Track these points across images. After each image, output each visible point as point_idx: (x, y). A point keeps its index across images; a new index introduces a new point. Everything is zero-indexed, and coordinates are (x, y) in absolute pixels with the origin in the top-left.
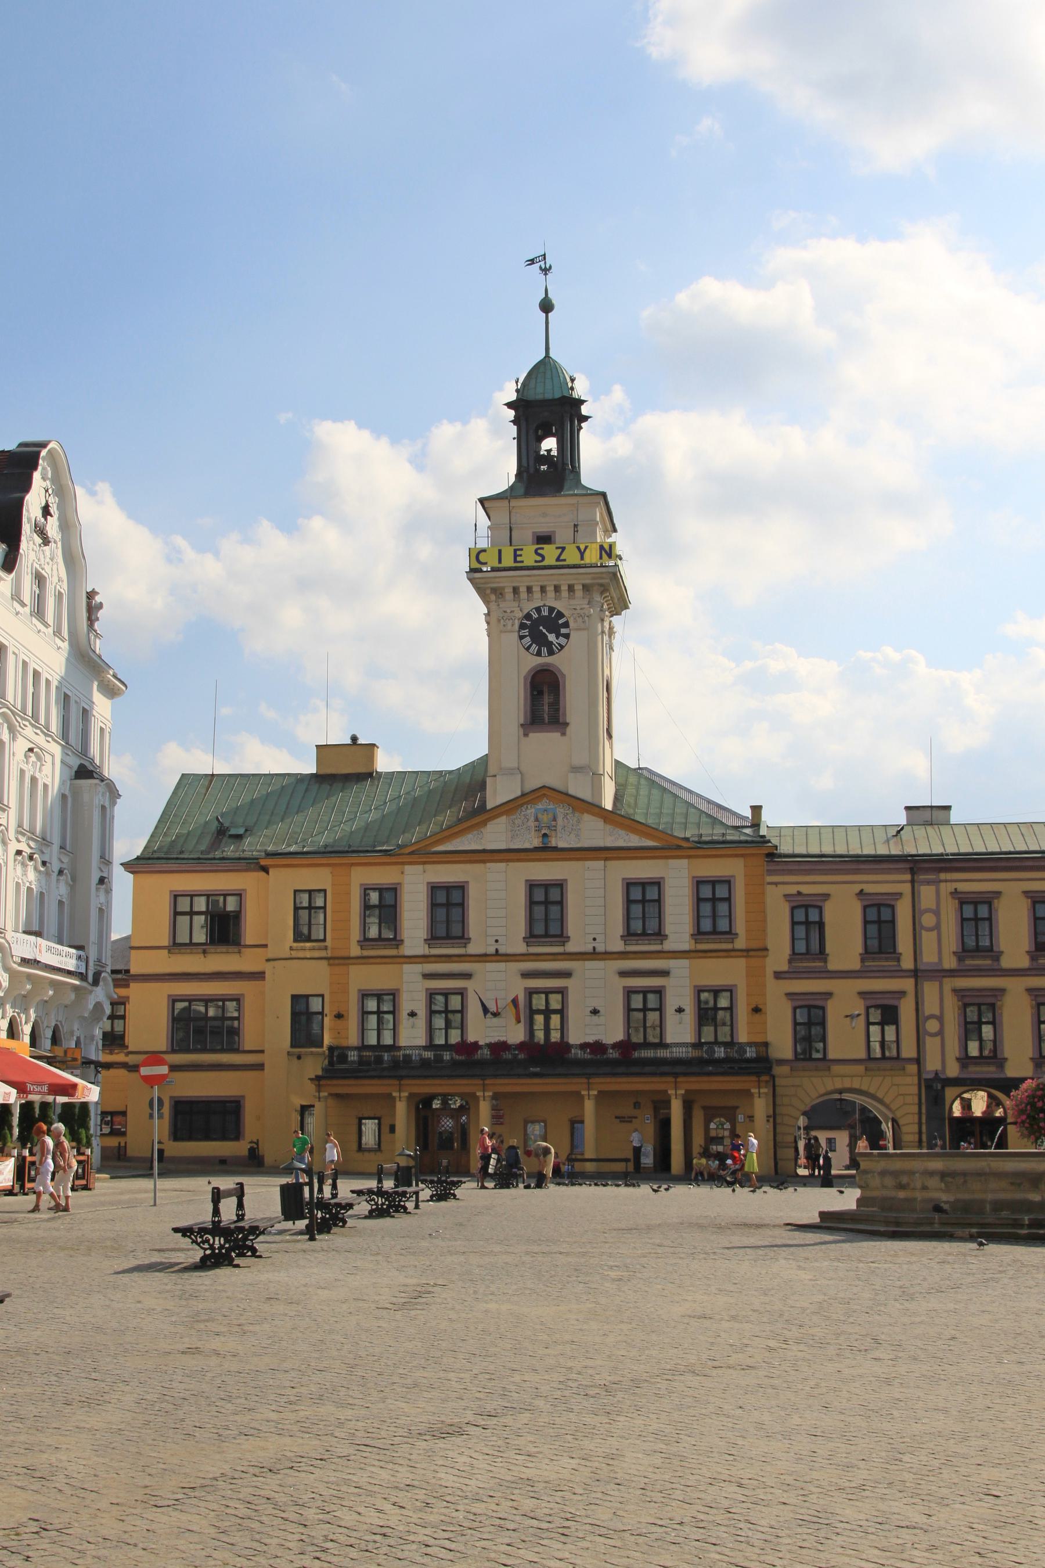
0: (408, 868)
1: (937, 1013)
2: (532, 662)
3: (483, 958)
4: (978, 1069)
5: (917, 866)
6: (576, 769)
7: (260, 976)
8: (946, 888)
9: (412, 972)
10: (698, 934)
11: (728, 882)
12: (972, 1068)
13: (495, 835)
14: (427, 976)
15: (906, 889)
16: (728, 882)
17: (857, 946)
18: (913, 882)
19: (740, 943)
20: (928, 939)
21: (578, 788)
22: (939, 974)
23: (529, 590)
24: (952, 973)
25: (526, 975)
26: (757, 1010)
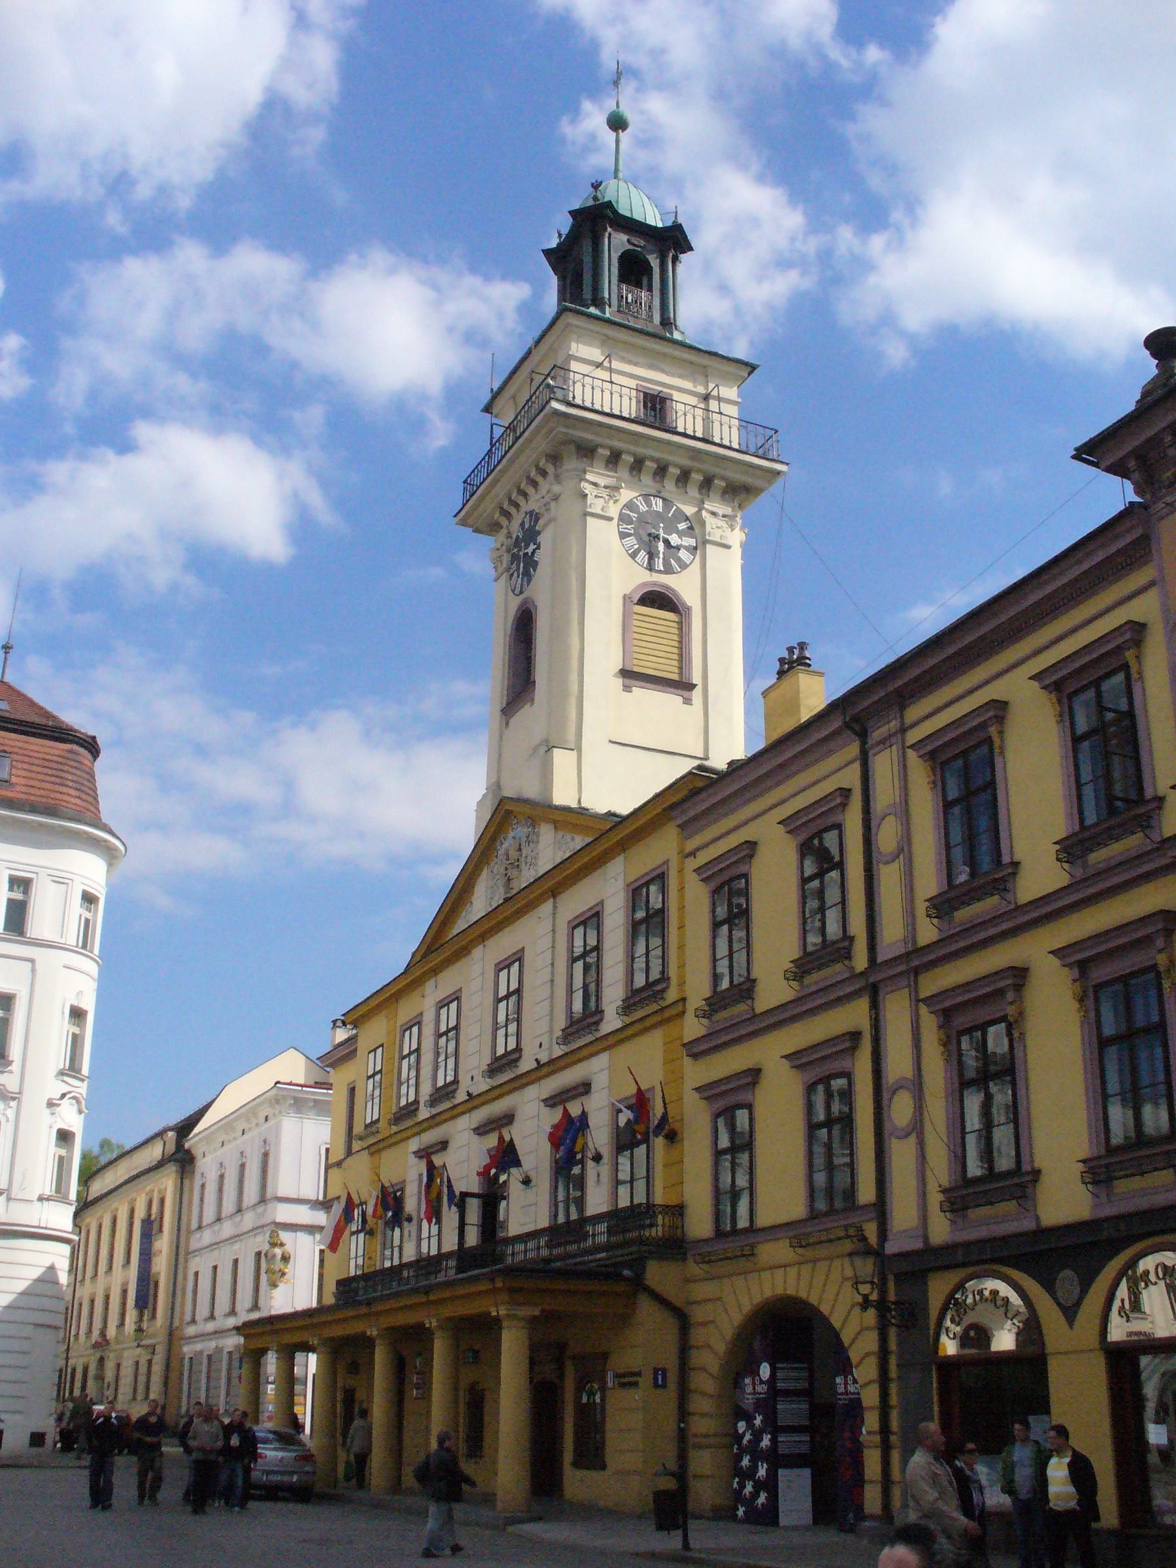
19: (672, 995)
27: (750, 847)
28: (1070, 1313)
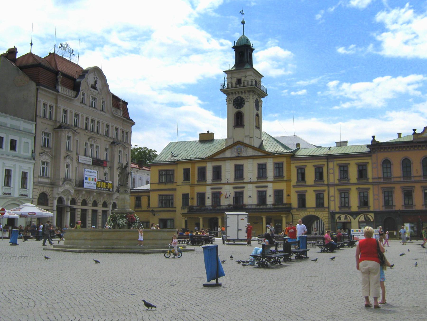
0: (208, 163)
1: (333, 195)
2: (236, 110)
3: (225, 184)
4: (344, 209)
5: (329, 158)
6: (246, 137)
7: (175, 189)
8: (336, 163)
9: (208, 188)
10: (275, 177)
11: (282, 163)
12: (342, 209)
13: (228, 154)
14: (212, 189)
15: (325, 163)
16: (282, 163)
17: (313, 178)
18: (327, 161)
19: (285, 178)
20: (331, 176)
21: (247, 141)
22: (334, 185)
23: (235, 92)
24: (337, 185)
25: (234, 188)
26: (288, 195)
27: (306, 166)
28: (355, 219)
